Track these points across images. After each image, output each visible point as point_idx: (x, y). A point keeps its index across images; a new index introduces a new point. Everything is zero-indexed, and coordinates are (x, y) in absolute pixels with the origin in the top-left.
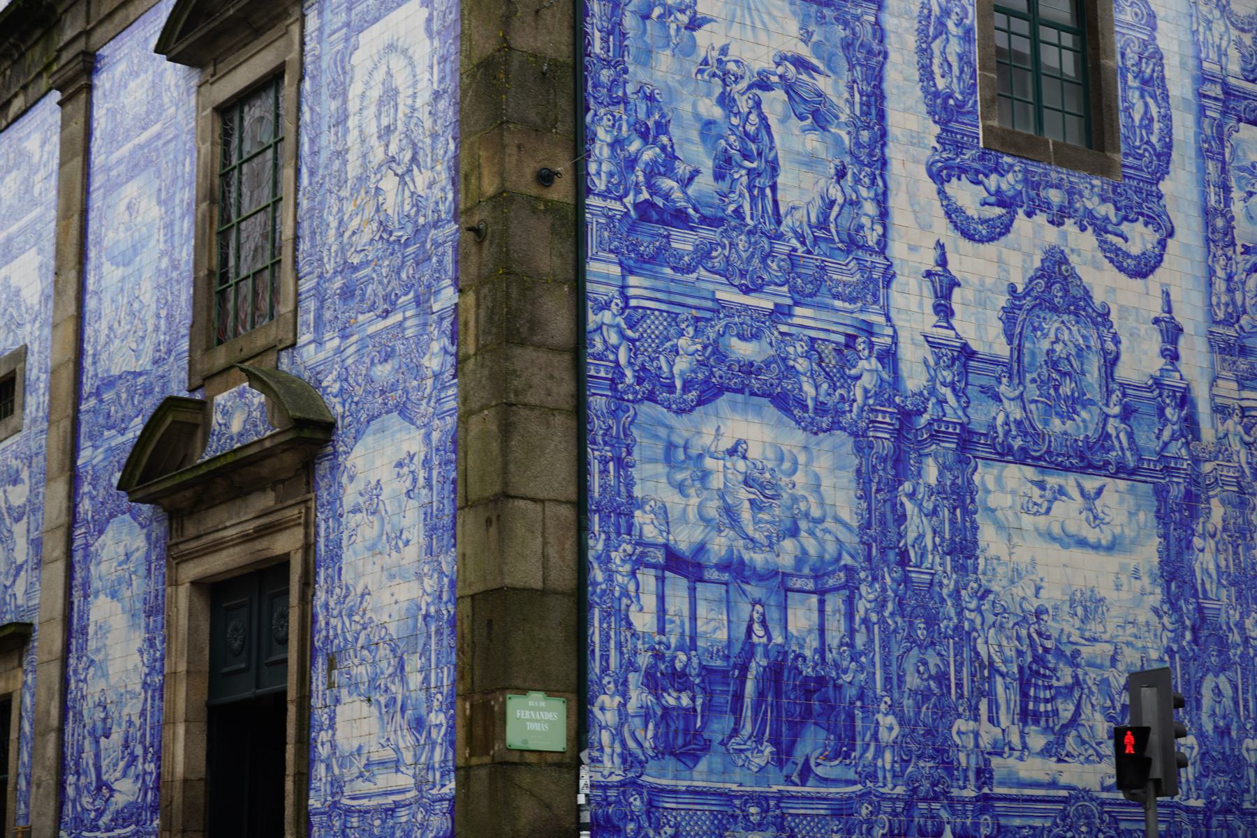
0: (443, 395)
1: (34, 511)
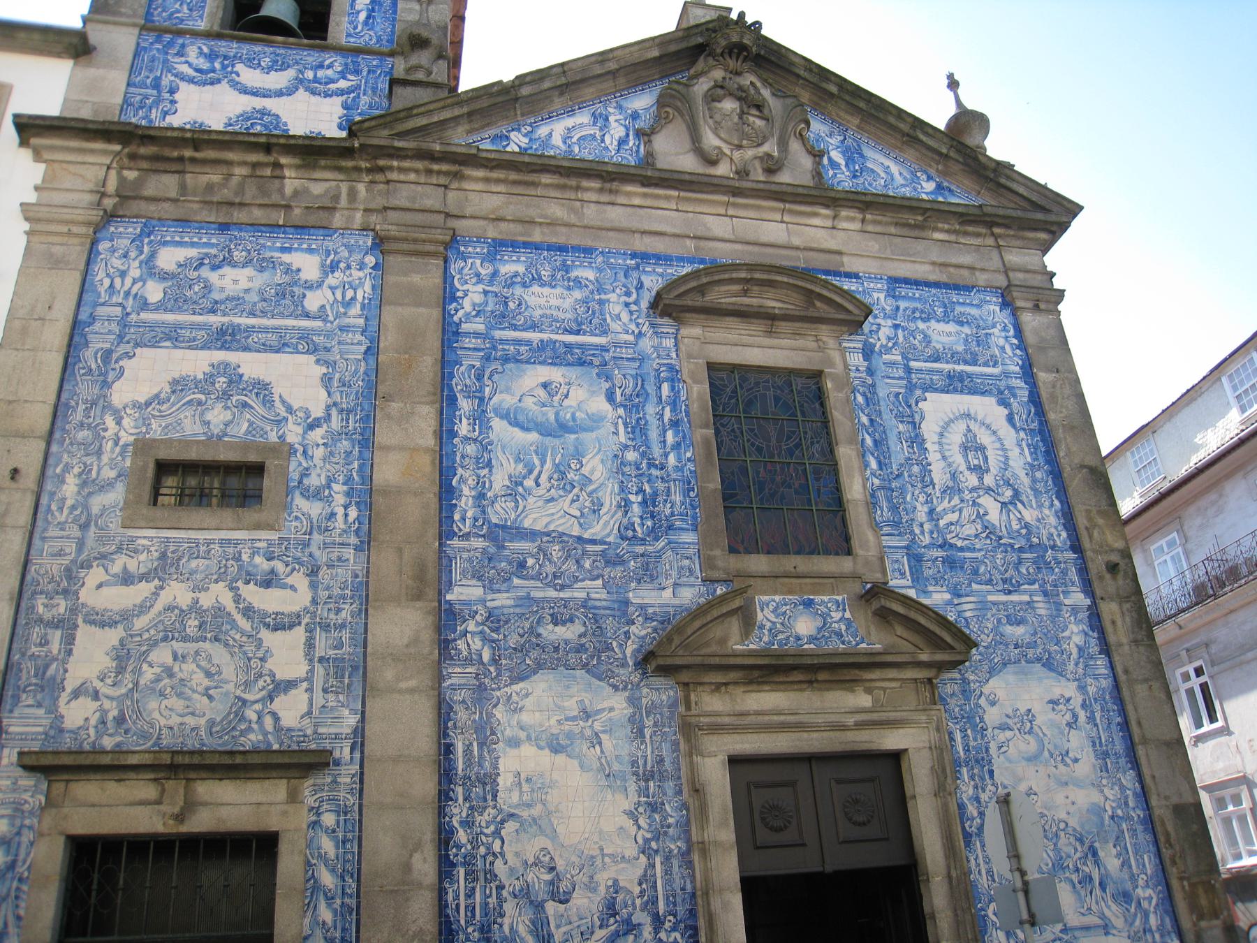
0: (1092, 663)
1: (326, 627)
